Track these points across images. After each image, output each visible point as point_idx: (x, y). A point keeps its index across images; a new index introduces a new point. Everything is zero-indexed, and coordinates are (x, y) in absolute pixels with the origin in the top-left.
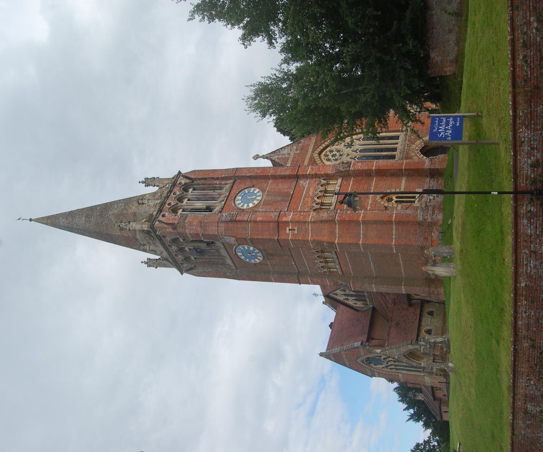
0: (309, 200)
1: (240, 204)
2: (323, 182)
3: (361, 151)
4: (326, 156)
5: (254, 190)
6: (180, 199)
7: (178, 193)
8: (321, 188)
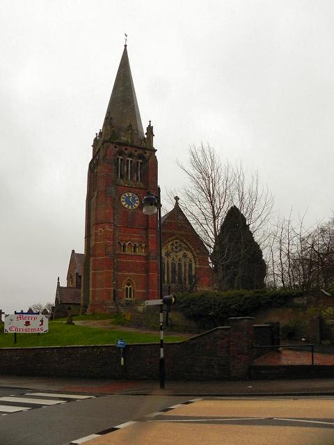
0: (128, 238)
1: (125, 196)
2: (144, 245)
3: (180, 264)
4: (176, 243)
5: (137, 203)
6: (131, 155)
7: (136, 154)
8: (137, 245)
